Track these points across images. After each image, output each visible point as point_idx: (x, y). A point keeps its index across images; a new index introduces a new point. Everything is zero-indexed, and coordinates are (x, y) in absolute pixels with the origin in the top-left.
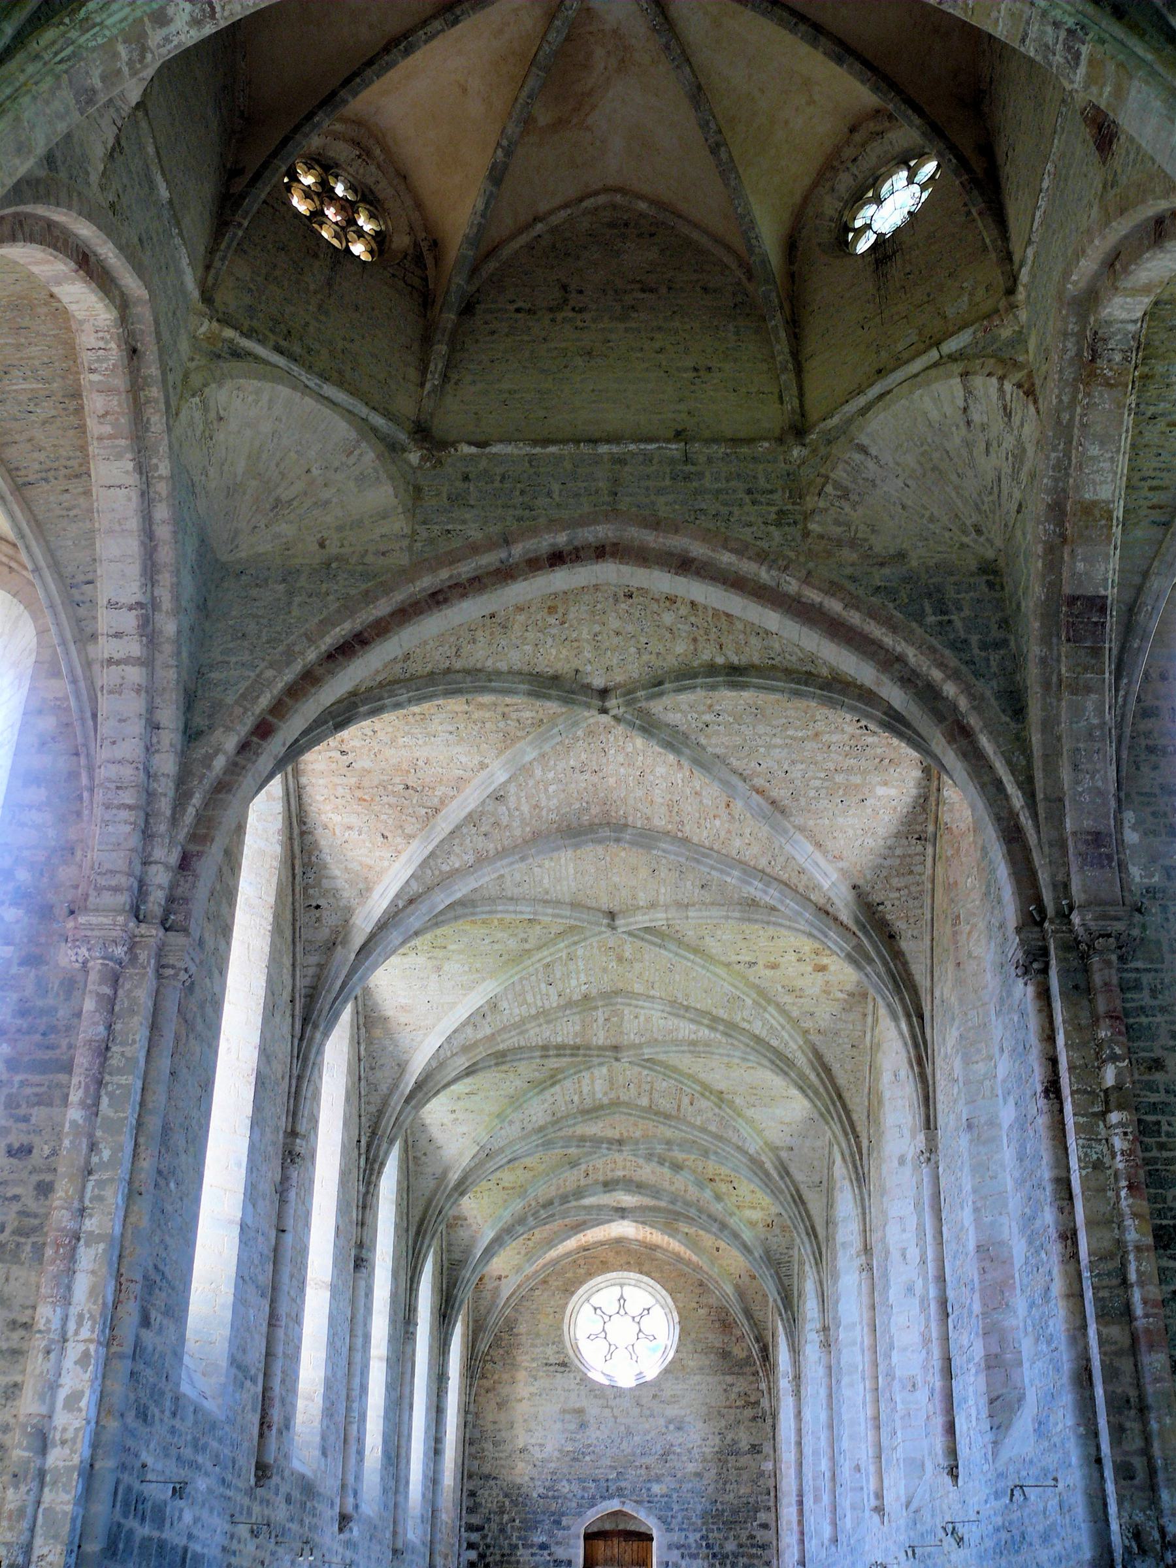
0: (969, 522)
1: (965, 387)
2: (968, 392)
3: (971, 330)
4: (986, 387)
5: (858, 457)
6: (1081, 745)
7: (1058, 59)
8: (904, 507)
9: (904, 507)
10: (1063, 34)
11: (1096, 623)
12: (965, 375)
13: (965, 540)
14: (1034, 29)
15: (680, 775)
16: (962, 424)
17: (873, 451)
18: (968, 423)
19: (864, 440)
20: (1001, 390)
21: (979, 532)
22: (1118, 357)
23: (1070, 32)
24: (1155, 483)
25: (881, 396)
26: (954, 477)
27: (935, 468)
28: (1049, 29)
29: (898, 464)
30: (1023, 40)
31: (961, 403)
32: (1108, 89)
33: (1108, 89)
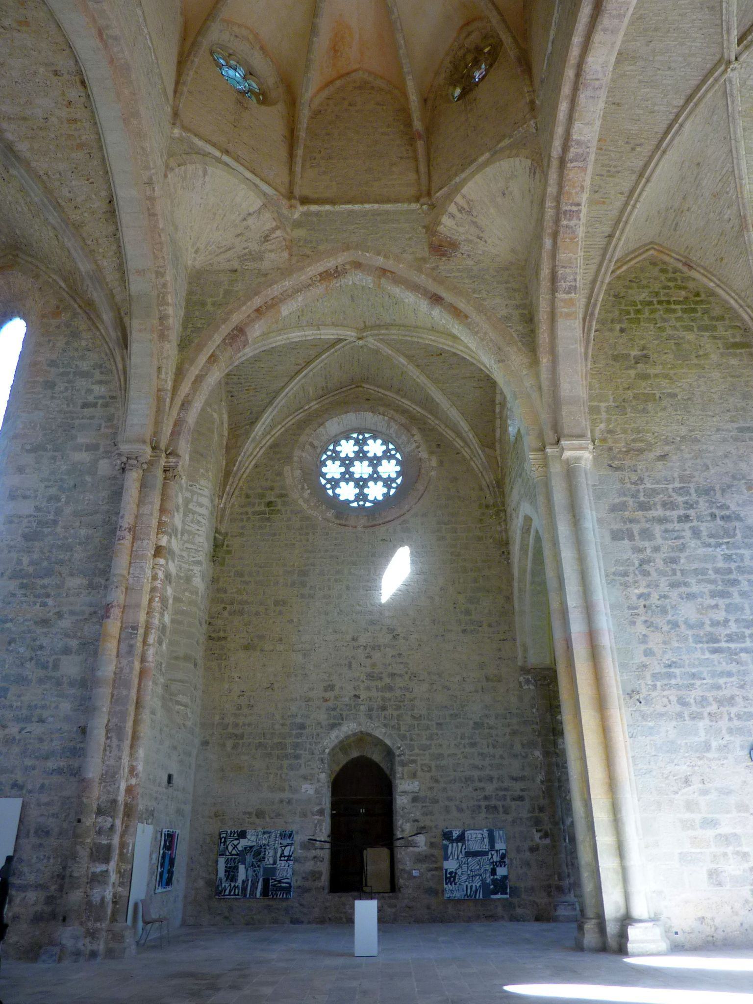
0: (198, 244)
1: (260, 209)
2: (259, 212)
3: (275, 192)
4: (267, 221)
5: (201, 173)
7: (564, 285)
9: (191, 211)
10: (573, 284)
12: (264, 206)
13: (190, 249)
14: (568, 270)
17: (207, 179)
18: (244, 219)
19: (210, 170)
20: (274, 230)
21: (196, 252)
22: (338, 285)
23: (576, 286)
25: (227, 164)
27: (215, 214)
28: (572, 277)
29: (207, 195)
30: (563, 267)
31: (251, 210)
32: (566, 310)
33: (566, 310)
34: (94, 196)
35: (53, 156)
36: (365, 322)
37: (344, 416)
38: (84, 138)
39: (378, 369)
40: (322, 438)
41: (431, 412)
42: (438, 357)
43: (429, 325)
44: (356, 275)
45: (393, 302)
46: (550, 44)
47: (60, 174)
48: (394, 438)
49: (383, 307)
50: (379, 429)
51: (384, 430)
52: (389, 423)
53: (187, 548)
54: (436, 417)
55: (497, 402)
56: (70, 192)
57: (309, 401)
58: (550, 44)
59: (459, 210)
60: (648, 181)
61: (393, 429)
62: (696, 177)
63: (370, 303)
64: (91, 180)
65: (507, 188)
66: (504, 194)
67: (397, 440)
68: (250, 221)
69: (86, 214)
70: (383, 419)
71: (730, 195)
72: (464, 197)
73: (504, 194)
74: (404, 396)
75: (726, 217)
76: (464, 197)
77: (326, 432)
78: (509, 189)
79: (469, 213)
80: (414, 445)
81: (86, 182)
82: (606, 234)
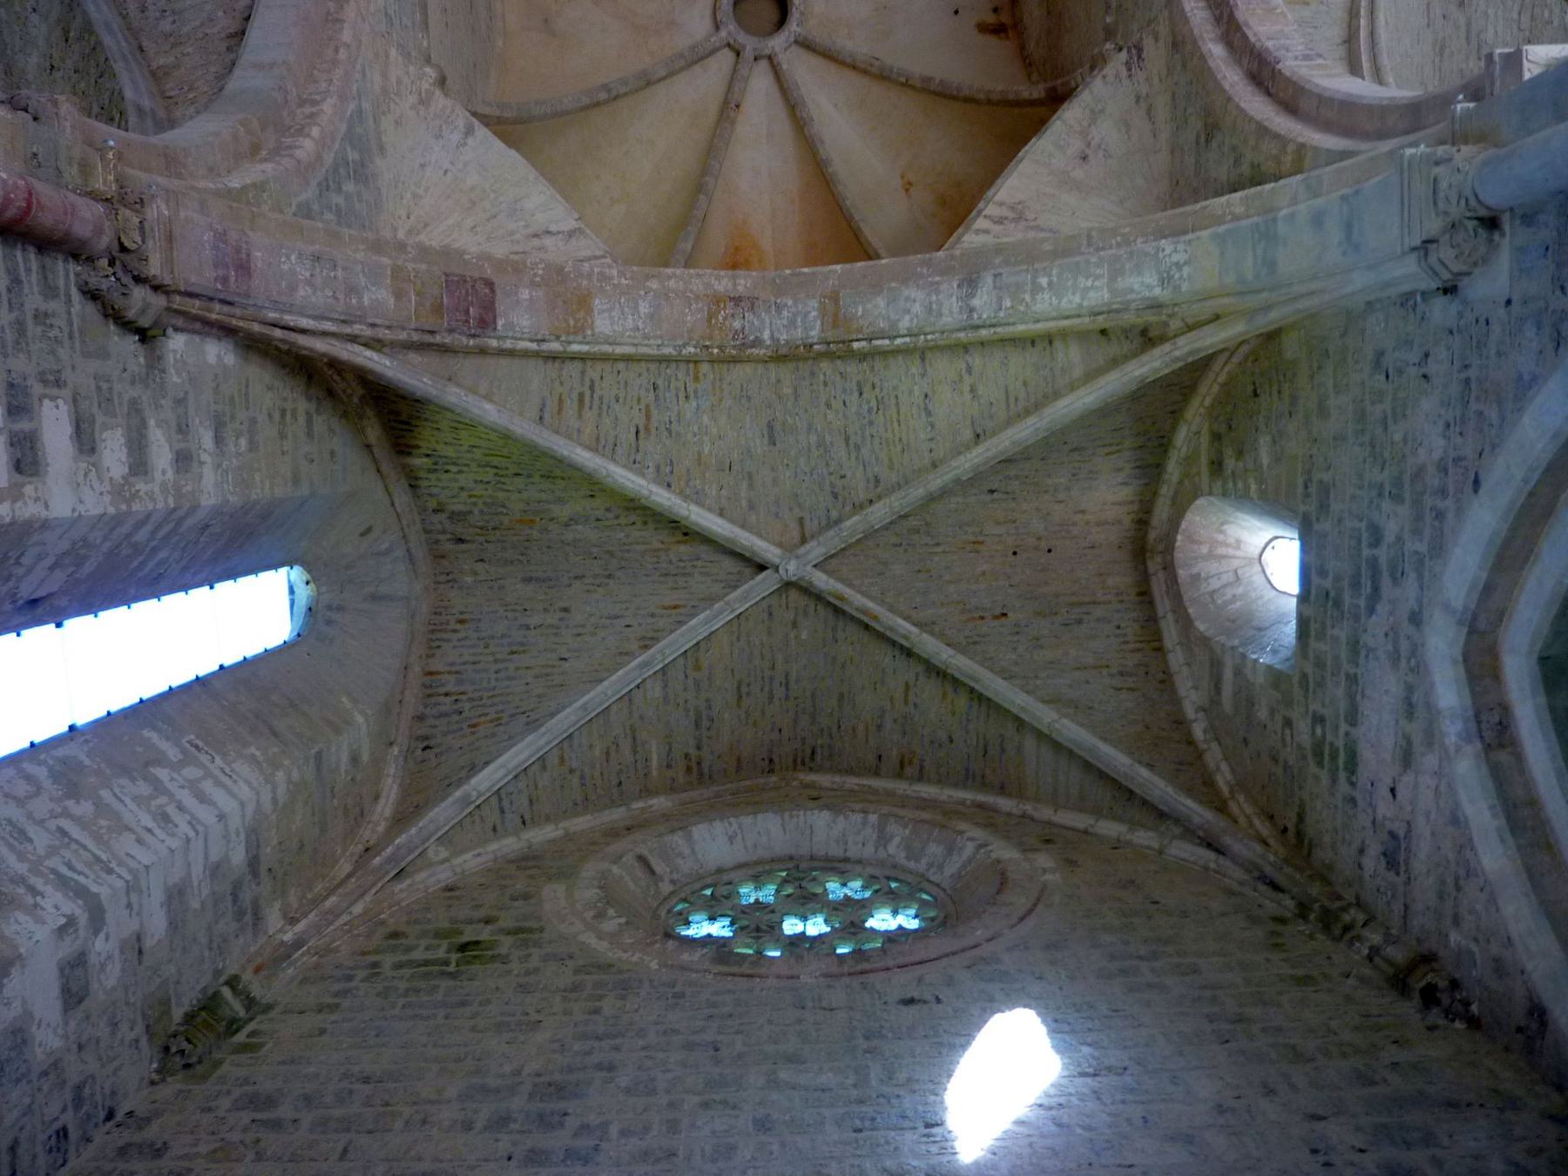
6: (340, 273)
8: (422, 166)
9: (422, 166)
11: (467, 312)
16: (530, 231)
17: (470, 141)
22: (737, 324)
24: (587, 399)
26: (469, 222)
29: (465, 165)
31: (553, 228)
34: (220, 14)
36: (801, 521)
37: (747, 820)
39: (841, 697)
40: (680, 861)
41: (1002, 790)
42: (996, 623)
43: (968, 434)
44: (779, 308)
45: (870, 410)
48: (903, 862)
49: (847, 440)
50: (853, 852)
51: (869, 851)
52: (881, 829)
53: (63, 833)
54: (1021, 796)
55: (1190, 713)
57: (647, 792)
59: (995, 223)
61: (897, 840)
62: (1468, 32)
63: (813, 438)
66: (1084, 158)
67: (912, 865)
68: (548, 241)
70: (865, 823)
71: (1556, 23)
73: (1084, 158)
74: (921, 777)
77: (693, 852)
78: (1093, 143)
80: (970, 848)
82: (1339, 40)
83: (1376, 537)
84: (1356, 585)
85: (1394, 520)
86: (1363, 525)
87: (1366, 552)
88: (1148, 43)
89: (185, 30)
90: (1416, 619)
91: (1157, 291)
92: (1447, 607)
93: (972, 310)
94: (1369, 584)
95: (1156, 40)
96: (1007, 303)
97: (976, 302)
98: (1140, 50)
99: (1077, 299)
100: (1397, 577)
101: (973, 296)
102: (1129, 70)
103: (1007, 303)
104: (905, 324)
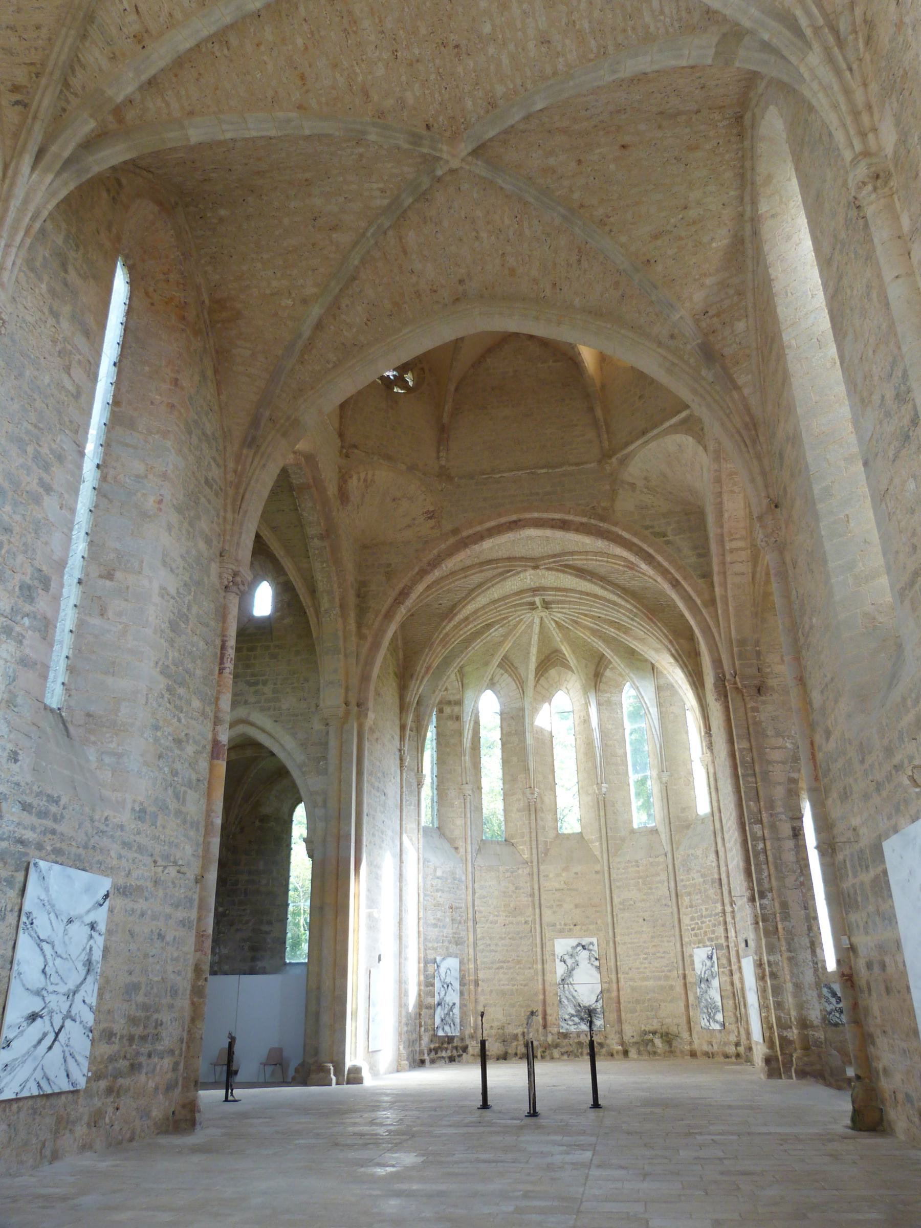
15: (360, 79)
34: (355, 330)
35: (376, 282)
38: (405, 306)
46: (500, 475)
47: (361, 292)
56: (347, 306)
58: (500, 475)
60: (465, 577)
64: (369, 323)
65: (399, 499)
66: (394, 500)
69: (332, 327)
72: (373, 475)
73: (394, 500)
75: (441, 602)
76: (373, 475)
79: (367, 487)
81: (365, 319)
83: (265, 683)
84: (253, 675)
85: (268, 690)
86: (267, 677)
87: (261, 678)
88: (432, 522)
89: (343, 317)
90: (246, 702)
91: (323, 609)
92: (249, 714)
93: (313, 538)
94: (252, 681)
95: (432, 528)
96: (317, 552)
97: (316, 540)
98: (430, 518)
99: (320, 578)
100: (256, 692)
101: (318, 539)
102: (426, 513)
103: (317, 552)
104: (305, 514)
